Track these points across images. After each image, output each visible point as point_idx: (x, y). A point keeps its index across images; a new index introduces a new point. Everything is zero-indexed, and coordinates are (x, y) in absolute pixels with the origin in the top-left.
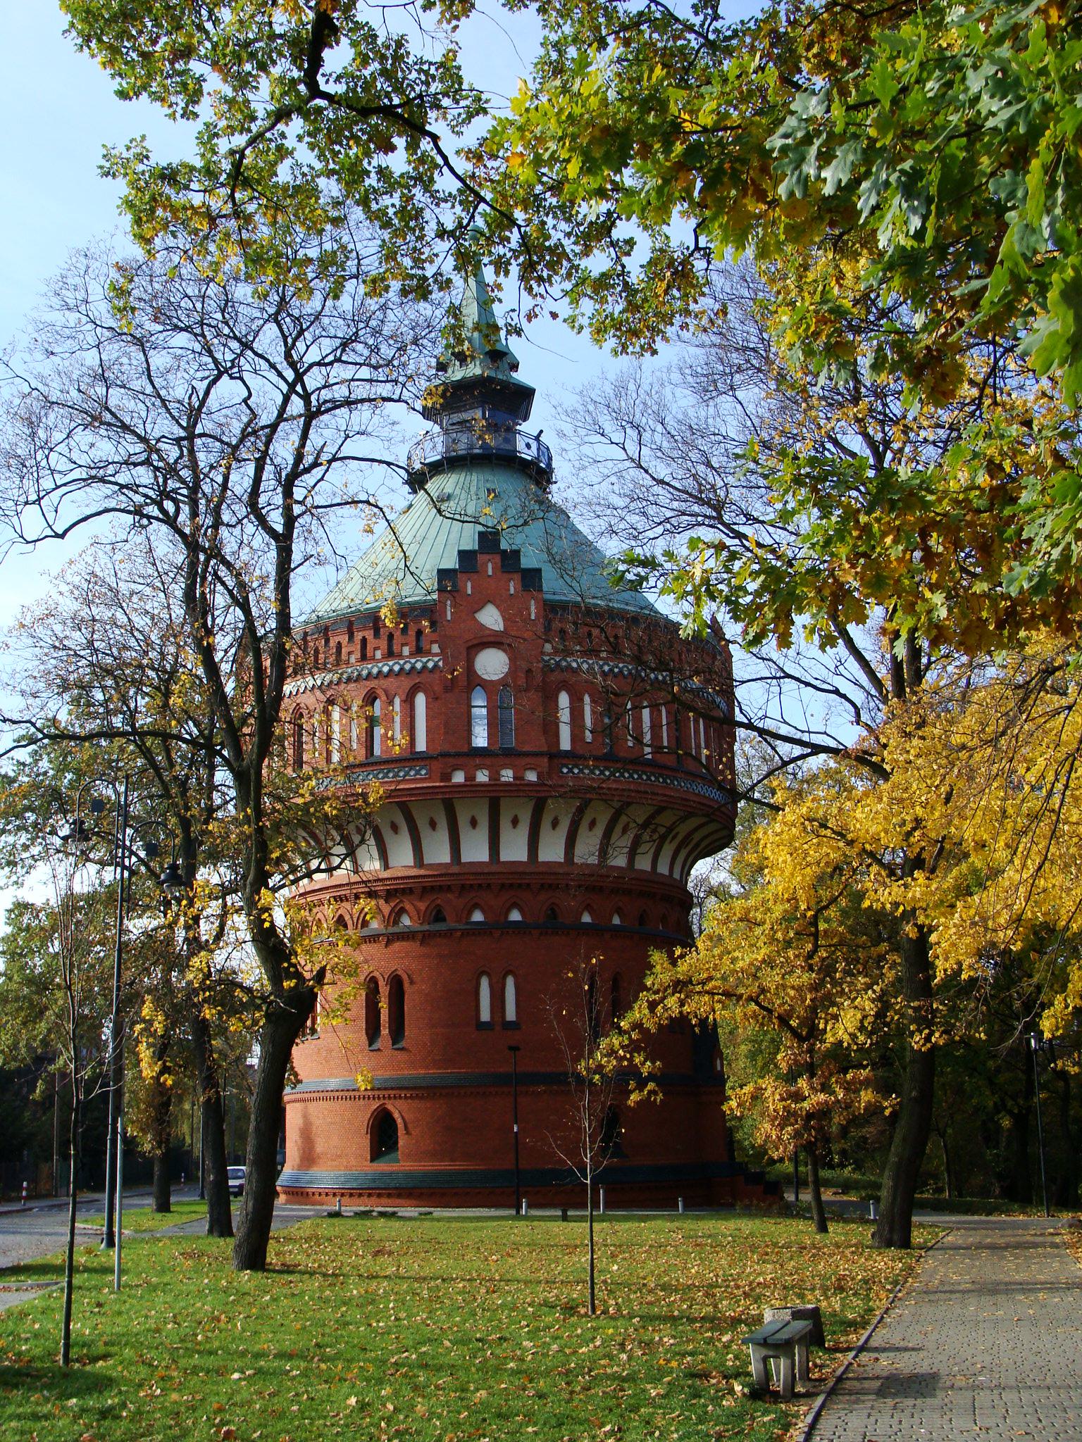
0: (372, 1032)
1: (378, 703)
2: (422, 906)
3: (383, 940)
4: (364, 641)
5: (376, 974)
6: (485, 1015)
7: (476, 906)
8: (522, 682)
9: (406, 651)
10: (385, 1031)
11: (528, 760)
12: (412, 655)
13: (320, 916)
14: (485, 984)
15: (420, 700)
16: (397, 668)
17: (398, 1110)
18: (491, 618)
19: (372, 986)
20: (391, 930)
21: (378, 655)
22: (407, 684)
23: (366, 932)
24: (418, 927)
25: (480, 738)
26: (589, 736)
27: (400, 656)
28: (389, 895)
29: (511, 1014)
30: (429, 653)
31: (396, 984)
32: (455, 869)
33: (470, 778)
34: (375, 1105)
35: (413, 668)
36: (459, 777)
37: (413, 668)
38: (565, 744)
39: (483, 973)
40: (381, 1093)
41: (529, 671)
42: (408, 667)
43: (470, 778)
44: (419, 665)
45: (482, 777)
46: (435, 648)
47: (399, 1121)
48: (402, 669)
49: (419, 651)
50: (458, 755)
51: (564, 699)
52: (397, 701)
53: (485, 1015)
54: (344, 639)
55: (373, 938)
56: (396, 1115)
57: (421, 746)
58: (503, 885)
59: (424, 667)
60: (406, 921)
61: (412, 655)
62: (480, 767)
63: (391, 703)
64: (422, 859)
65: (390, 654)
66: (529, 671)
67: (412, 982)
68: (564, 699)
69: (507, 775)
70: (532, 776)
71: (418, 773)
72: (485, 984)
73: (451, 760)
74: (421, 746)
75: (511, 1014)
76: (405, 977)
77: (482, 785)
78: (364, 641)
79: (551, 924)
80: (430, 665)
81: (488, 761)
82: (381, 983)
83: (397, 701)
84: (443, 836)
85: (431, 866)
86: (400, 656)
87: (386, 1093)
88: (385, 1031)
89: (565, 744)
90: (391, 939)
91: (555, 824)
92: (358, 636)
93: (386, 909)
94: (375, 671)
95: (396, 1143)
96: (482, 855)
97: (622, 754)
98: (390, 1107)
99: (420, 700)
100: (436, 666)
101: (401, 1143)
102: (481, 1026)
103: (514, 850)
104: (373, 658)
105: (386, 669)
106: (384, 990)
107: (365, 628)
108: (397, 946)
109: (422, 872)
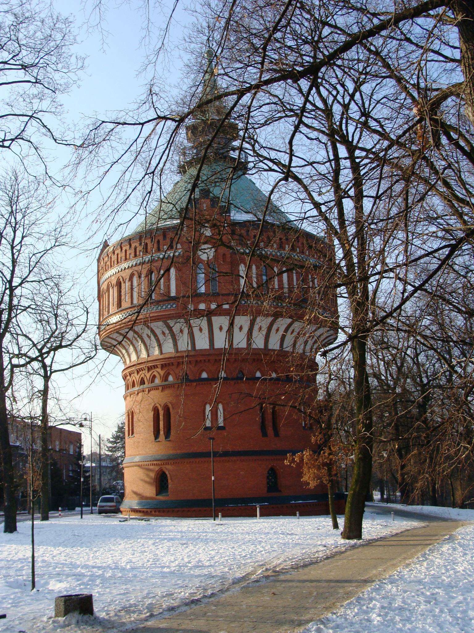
0: (156, 434)
1: (153, 274)
3: (160, 388)
5: (157, 405)
13: (134, 378)
17: (169, 469)
19: (156, 410)
20: (164, 383)
22: (166, 263)
23: (153, 385)
28: (163, 366)
31: (167, 410)
32: (193, 353)
34: (157, 468)
45: (202, 306)
47: (168, 476)
49: (171, 247)
53: (208, 424)
54: (137, 244)
55: (156, 388)
56: (167, 473)
57: (173, 294)
60: (171, 378)
62: (200, 302)
67: (173, 408)
69: (213, 306)
71: (172, 306)
76: (170, 406)
78: (146, 244)
82: (160, 409)
85: (181, 352)
88: (162, 432)
90: (164, 388)
93: (162, 373)
95: (167, 486)
96: (206, 346)
98: (165, 470)
99: (173, 271)
101: (170, 486)
106: (161, 413)
108: (166, 392)
109: (178, 355)
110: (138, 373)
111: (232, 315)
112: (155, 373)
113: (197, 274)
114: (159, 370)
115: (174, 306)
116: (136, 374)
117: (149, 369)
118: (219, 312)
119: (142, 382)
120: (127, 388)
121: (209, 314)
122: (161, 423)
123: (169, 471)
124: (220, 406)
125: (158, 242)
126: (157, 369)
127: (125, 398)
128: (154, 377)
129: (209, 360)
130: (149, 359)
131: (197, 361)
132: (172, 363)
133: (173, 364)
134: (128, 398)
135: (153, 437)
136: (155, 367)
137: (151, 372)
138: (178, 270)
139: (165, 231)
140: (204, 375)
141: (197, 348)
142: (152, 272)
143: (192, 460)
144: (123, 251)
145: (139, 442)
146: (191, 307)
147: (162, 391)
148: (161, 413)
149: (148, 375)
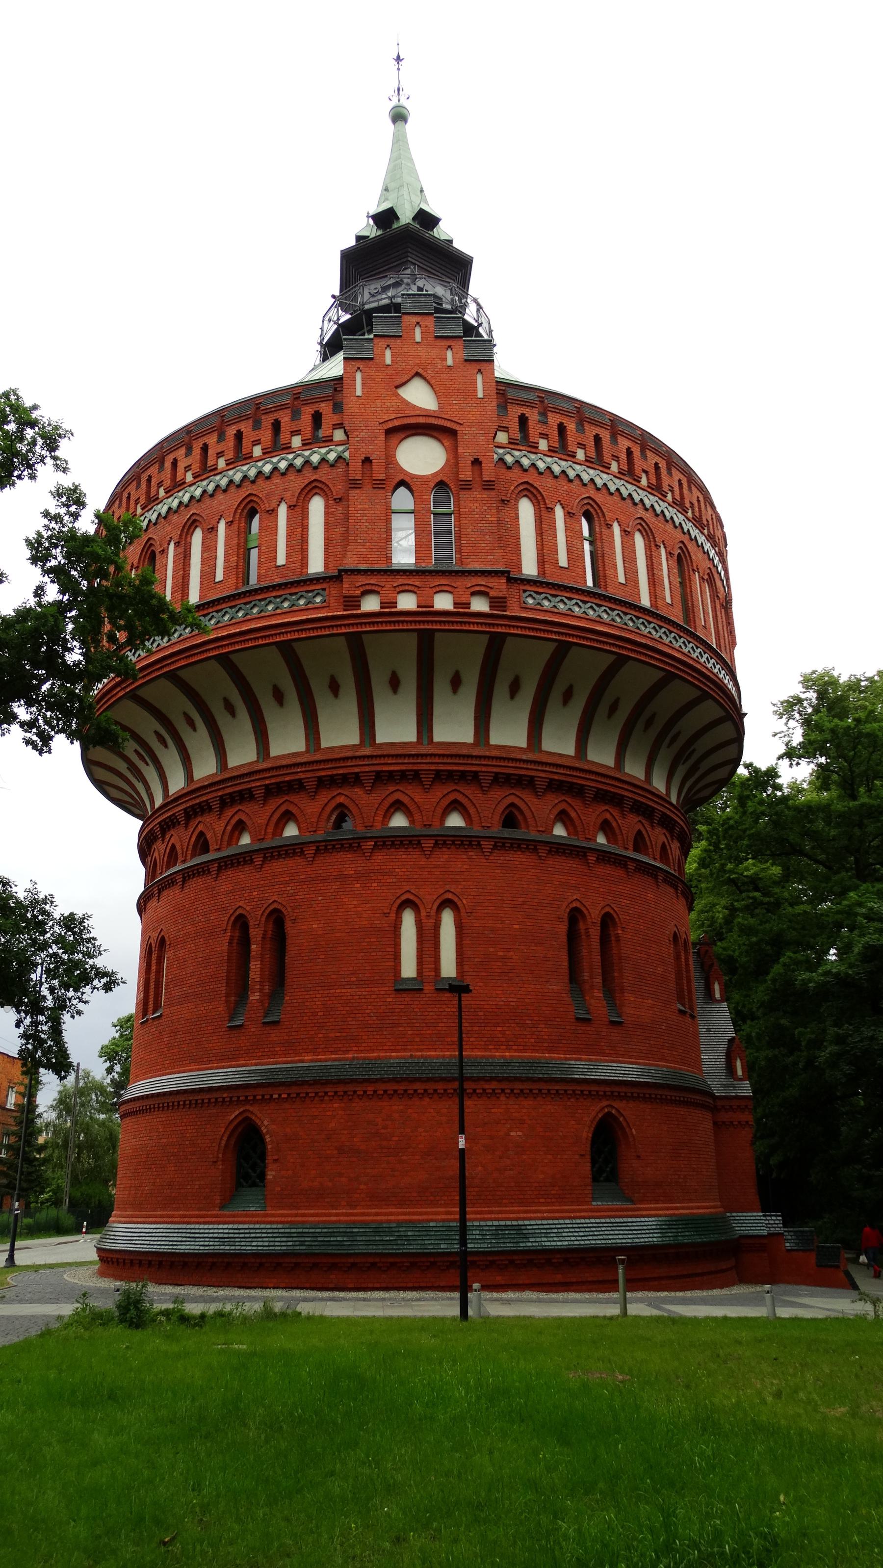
4: (239, 436)
6: (409, 968)
7: (398, 806)
8: (466, 473)
9: (296, 441)
14: (408, 920)
15: (317, 507)
16: (283, 465)
18: (419, 396)
21: (257, 451)
22: (297, 483)
24: (308, 837)
25: (404, 551)
26: (563, 561)
27: (287, 448)
29: (448, 968)
30: (328, 440)
32: (367, 751)
34: (234, 1113)
35: (307, 462)
36: (371, 604)
37: (307, 462)
38: (529, 567)
39: (408, 903)
41: (477, 462)
42: (299, 462)
44: (315, 459)
45: (407, 602)
46: (339, 435)
51: (526, 510)
52: (283, 510)
53: (409, 968)
57: (316, 565)
58: (438, 773)
59: (323, 460)
61: (306, 444)
63: (273, 512)
65: (277, 447)
66: (477, 462)
68: (526, 510)
69: (443, 602)
70: (479, 605)
72: (408, 920)
73: (362, 580)
74: (316, 565)
75: (448, 968)
79: (511, 837)
80: (332, 457)
83: (283, 510)
84: (349, 704)
86: (287, 448)
88: (255, 997)
89: (529, 567)
91: (514, 689)
94: (252, 473)
97: (611, 592)
99: (317, 507)
100: (339, 457)
103: (454, 728)
105: (267, 468)
107: (240, 419)
109: (318, 757)
113: (389, 513)
115: (318, 599)
117: (225, 802)
119: (202, 845)
120: (150, 876)
122: (255, 967)
125: (276, 426)
127: (142, 905)
128: (240, 827)
134: (152, 904)
136: (245, 796)
137: (229, 813)
138: (334, 501)
139: (296, 397)
142: (252, 513)
144: (168, 465)
148: (256, 933)
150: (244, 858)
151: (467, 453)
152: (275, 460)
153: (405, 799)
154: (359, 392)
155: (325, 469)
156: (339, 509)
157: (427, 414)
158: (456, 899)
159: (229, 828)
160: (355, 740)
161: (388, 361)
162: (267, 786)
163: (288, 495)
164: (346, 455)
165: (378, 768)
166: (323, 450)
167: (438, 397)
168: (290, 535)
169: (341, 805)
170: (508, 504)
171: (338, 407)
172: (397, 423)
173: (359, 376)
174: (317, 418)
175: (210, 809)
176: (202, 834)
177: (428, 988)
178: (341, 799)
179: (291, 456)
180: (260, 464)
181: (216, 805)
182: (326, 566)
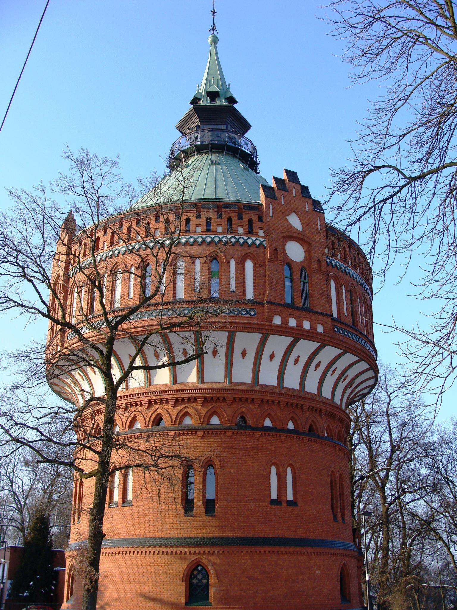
2: (230, 411)
3: (200, 434)
4: (209, 219)
7: (269, 416)
8: (315, 266)
10: (198, 503)
11: (321, 317)
12: (245, 233)
14: (273, 470)
15: (249, 265)
17: (212, 563)
20: (205, 426)
22: (241, 252)
27: (236, 233)
28: (206, 401)
29: (290, 496)
33: (285, 322)
36: (277, 320)
37: (246, 242)
40: (197, 550)
42: (241, 241)
43: (285, 322)
44: (250, 241)
46: (261, 233)
47: (212, 571)
48: (237, 241)
49: (250, 232)
50: (279, 305)
52: (232, 263)
53: (274, 495)
55: (192, 431)
59: (254, 243)
61: (245, 233)
64: (231, 378)
72: (273, 470)
74: (250, 294)
77: (292, 328)
78: (209, 219)
80: (258, 242)
81: (296, 313)
83: (232, 263)
87: (202, 550)
88: (198, 503)
92: (204, 215)
93: (203, 411)
98: (204, 561)
99: (249, 265)
100: (261, 244)
102: (273, 502)
104: (215, 232)
108: (211, 440)
109: (233, 387)
110: (150, 404)
111: (324, 341)
112: (189, 410)
114: (198, 406)
116: (144, 408)
118: (311, 336)
121: (298, 335)
123: (214, 564)
124: (289, 471)
126: (194, 405)
129: (279, 402)
130: (175, 387)
131: (262, 401)
132: (224, 398)
133: (224, 398)
135: (180, 508)
138: (259, 266)
140: (268, 423)
141: (260, 383)
143: (253, 549)
145: (145, 516)
146: (277, 320)
147: (202, 438)
149: (174, 412)
150: (192, 431)
151: (315, 256)
152: (229, 236)
153: (273, 414)
154: (271, 215)
155: (253, 249)
156: (261, 270)
157: (298, 232)
158: (294, 464)
159: (180, 415)
160: (250, 381)
161: (283, 203)
162: (205, 398)
163: (236, 256)
164: (264, 243)
165: (263, 397)
166: (254, 239)
167: (302, 226)
168: (236, 278)
169: (242, 412)
170: (327, 281)
171: (260, 219)
172: (288, 234)
173: (271, 206)
174: (250, 221)
175: (167, 401)
176: (159, 414)
177: (284, 504)
178: (244, 410)
179: (237, 237)
180: (221, 236)
181: (172, 402)
182: (255, 296)
